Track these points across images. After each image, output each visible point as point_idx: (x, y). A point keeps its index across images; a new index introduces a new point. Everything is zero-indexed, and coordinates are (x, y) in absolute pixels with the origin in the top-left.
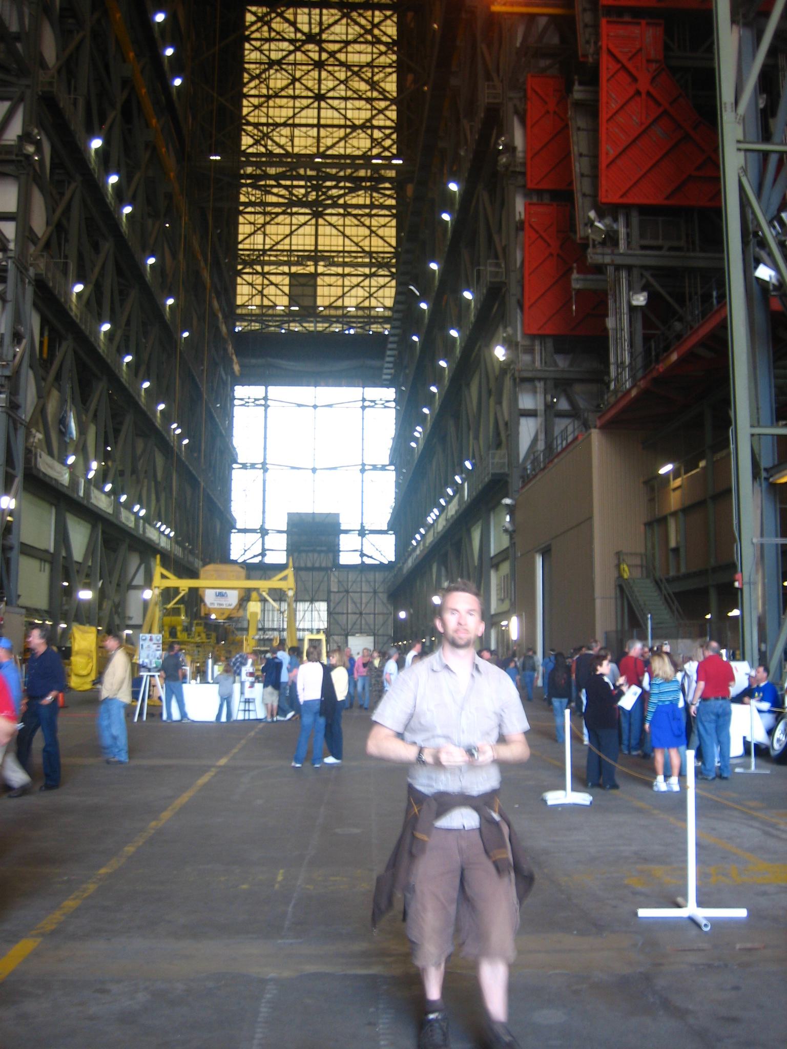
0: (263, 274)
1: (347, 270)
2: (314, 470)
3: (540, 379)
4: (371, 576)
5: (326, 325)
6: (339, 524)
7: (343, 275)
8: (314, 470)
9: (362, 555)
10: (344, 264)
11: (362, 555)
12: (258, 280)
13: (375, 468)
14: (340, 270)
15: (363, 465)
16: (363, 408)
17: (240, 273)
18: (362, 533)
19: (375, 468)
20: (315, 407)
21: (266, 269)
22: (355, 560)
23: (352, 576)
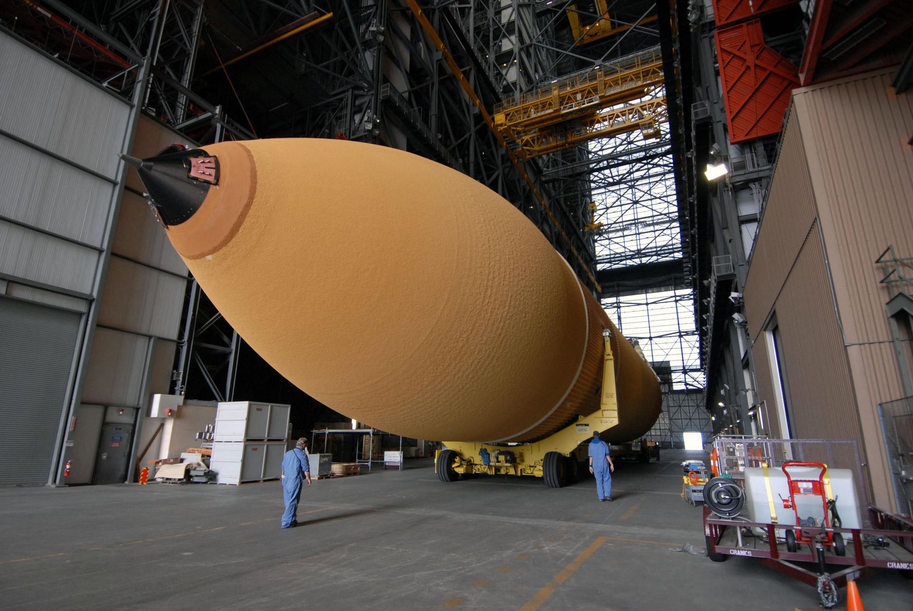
0: (609, 239)
1: (657, 227)
2: (651, 338)
3: (754, 181)
4: (694, 396)
5: (648, 258)
6: (670, 367)
7: (654, 231)
8: (651, 338)
9: (686, 384)
10: (653, 224)
11: (686, 384)
12: (606, 242)
13: (687, 334)
14: (651, 228)
15: (680, 332)
16: (676, 301)
17: (596, 241)
18: (685, 371)
19: (687, 334)
20: (647, 304)
21: (611, 235)
22: (682, 387)
23: (682, 397)
